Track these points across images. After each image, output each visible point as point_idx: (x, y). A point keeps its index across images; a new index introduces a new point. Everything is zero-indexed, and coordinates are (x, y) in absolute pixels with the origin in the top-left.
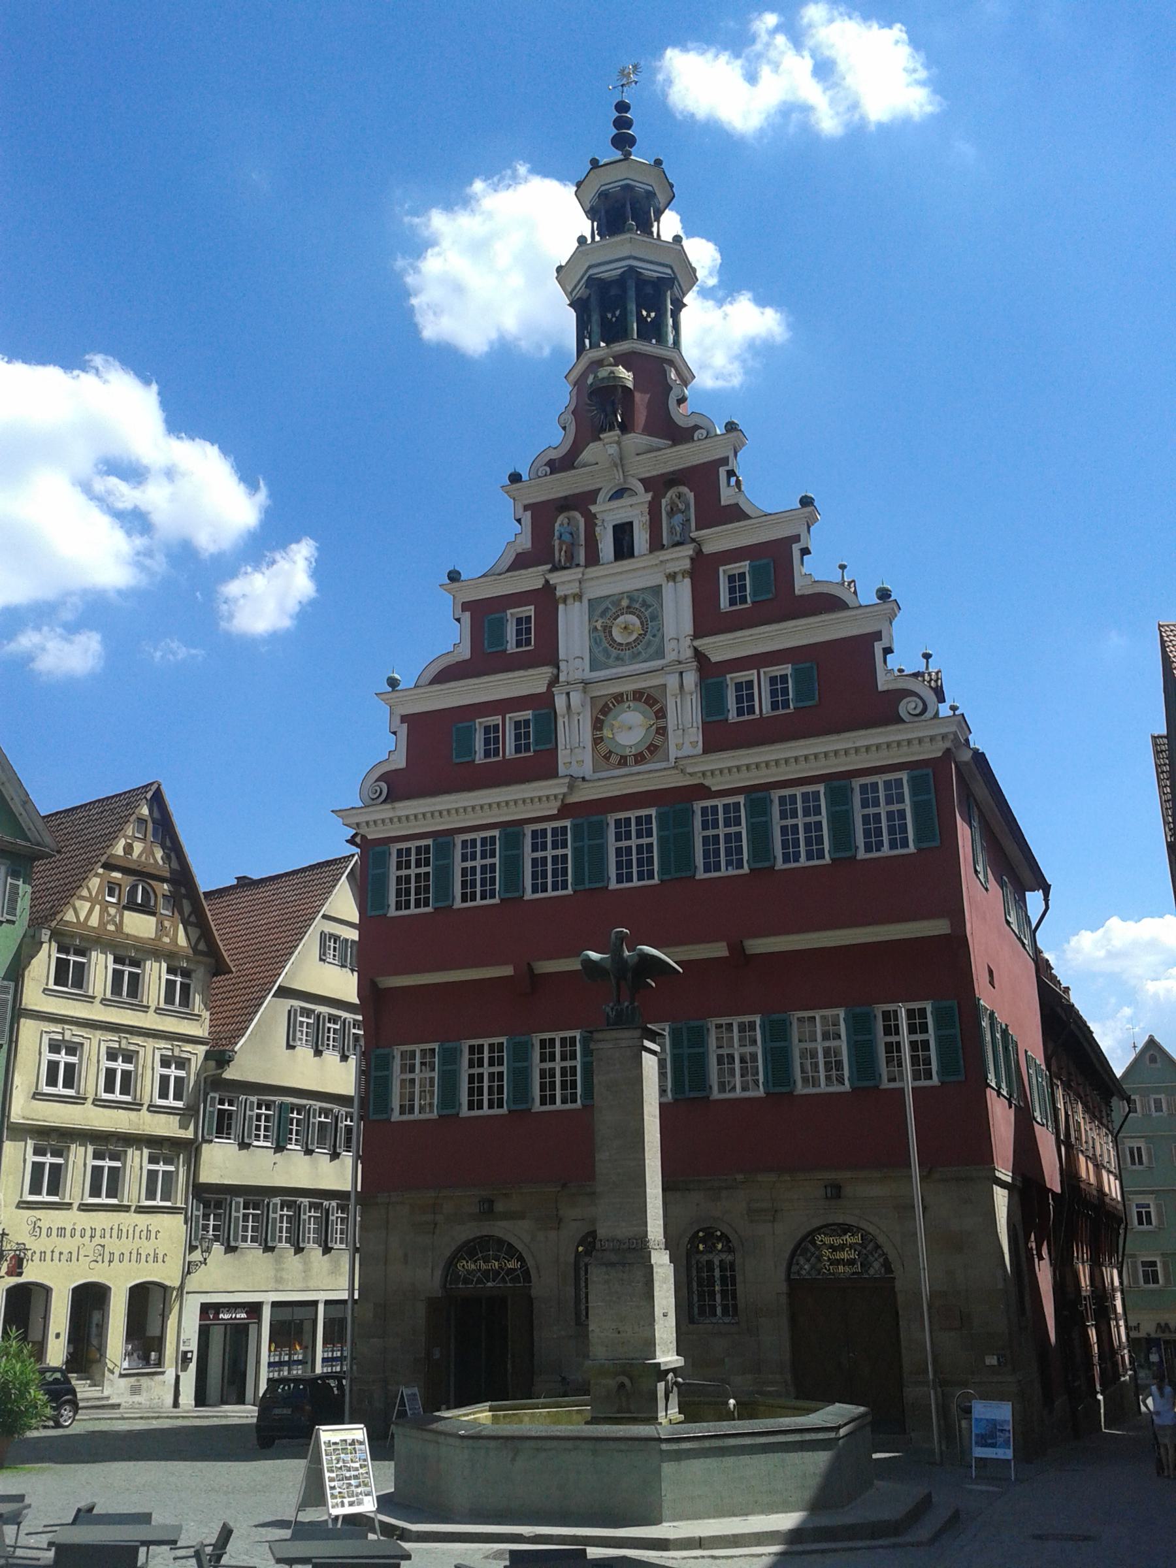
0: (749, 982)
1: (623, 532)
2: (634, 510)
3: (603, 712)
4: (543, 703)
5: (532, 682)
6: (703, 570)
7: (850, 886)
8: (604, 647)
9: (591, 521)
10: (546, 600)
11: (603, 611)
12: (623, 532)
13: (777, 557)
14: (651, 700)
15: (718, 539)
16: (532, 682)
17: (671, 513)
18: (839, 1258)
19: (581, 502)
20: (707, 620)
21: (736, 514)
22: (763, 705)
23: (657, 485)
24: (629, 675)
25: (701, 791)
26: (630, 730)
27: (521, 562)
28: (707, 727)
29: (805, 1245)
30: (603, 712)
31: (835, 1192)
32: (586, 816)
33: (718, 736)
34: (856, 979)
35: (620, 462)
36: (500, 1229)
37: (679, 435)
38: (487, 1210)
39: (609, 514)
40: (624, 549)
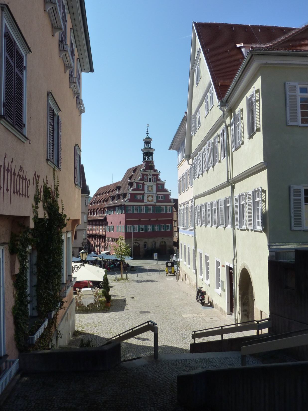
0: (157, 222)
1: (150, 179)
2: (151, 177)
3: (148, 196)
4: (143, 194)
5: (142, 192)
6: (157, 185)
7: (166, 215)
8: (148, 191)
9: (147, 177)
10: (143, 184)
11: (148, 186)
12: (150, 179)
13: (163, 185)
14: (152, 196)
15: (158, 182)
16: (142, 192)
17: (155, 179)
18: (163, 243)
19: (147, 175)
20: (157, 190)
21: (159, 180)
22: (161, 199)
23: (153, 175)
24: (151, 193)
25: (156, 205)
26: (150, 198)
27: (140, 180)
28: (157, 200)
29: (161, 243)
30: (148, 196)
31: (163, 238)
32: (146, 206)
33: (158, 201)
34: (165, 222)
35: (150, 172)
36: (137, 241)
37: (155, 171)
38: (136, 240)
39: (149, 177)
40: (150, 181)
